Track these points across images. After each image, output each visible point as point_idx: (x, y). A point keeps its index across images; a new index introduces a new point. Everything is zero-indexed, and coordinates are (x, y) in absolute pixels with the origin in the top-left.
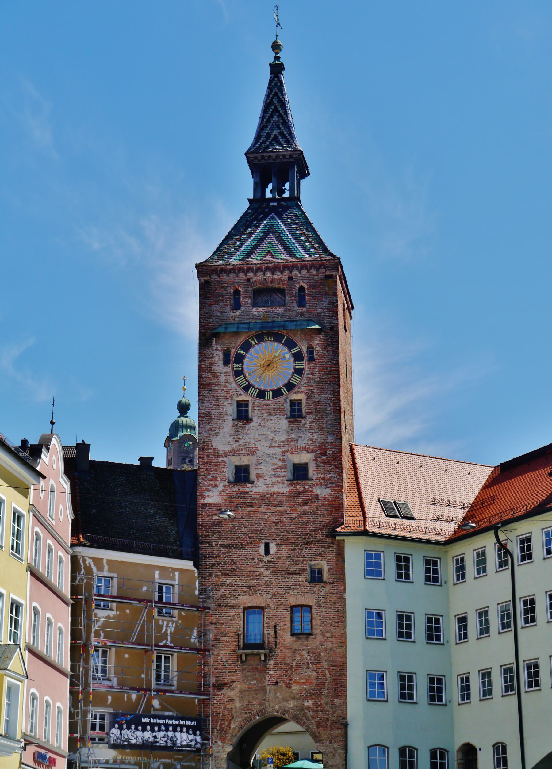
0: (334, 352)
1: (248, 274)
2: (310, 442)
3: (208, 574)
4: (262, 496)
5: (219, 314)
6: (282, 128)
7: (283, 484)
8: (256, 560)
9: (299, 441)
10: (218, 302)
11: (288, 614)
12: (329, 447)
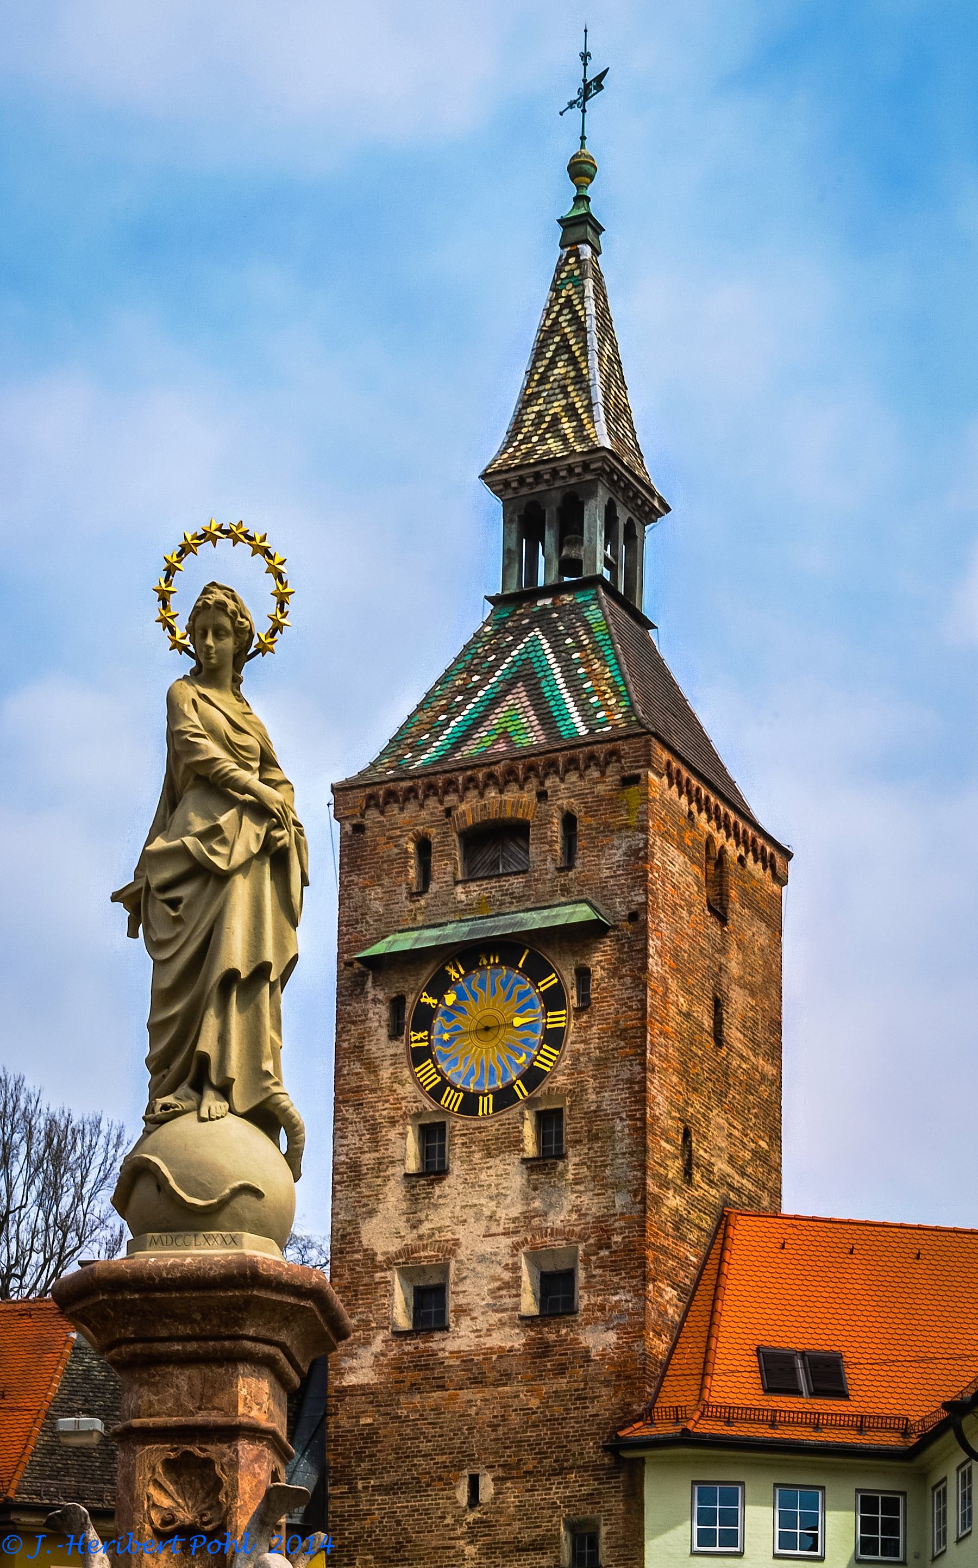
1: (447, 798)
2: (575, 1216)
3: (346, 1560)
4: (466, 1360)
7: (513, 1327)
8: (449, 1520)
9: (551, 1217)
10: (379, 878)
12: (617, 1224)
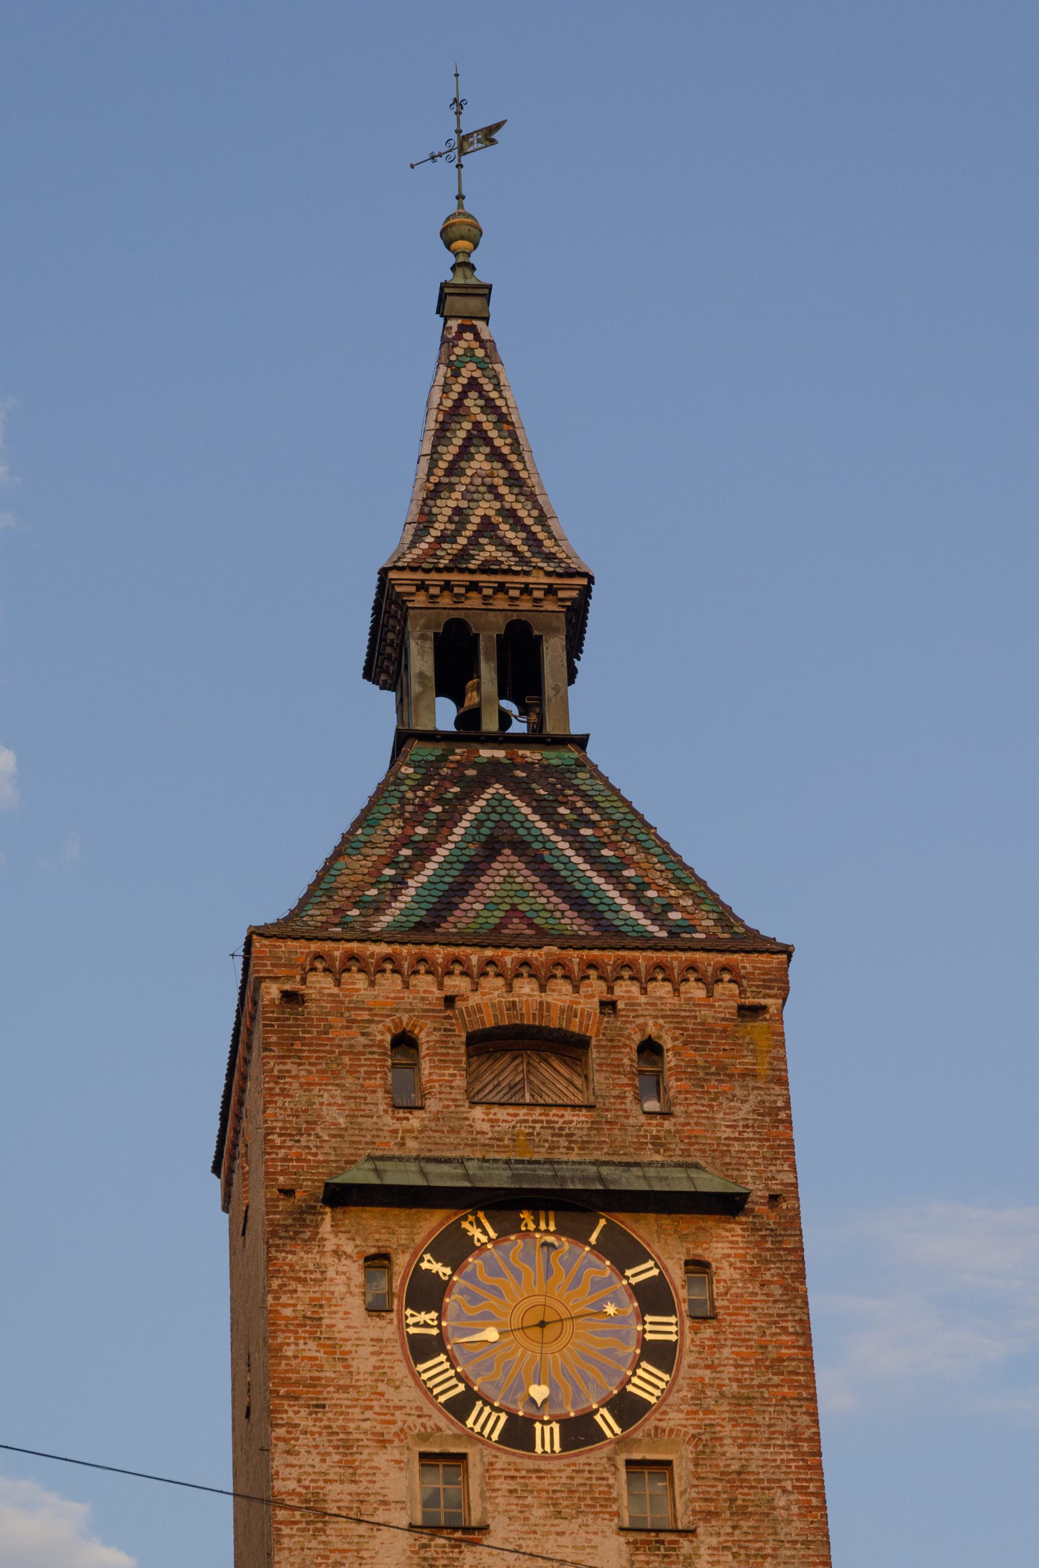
0: (786, 1288)
1: (448, 981)
5: (342, 1121)
6: (510, 498)
10: (336, 1074)
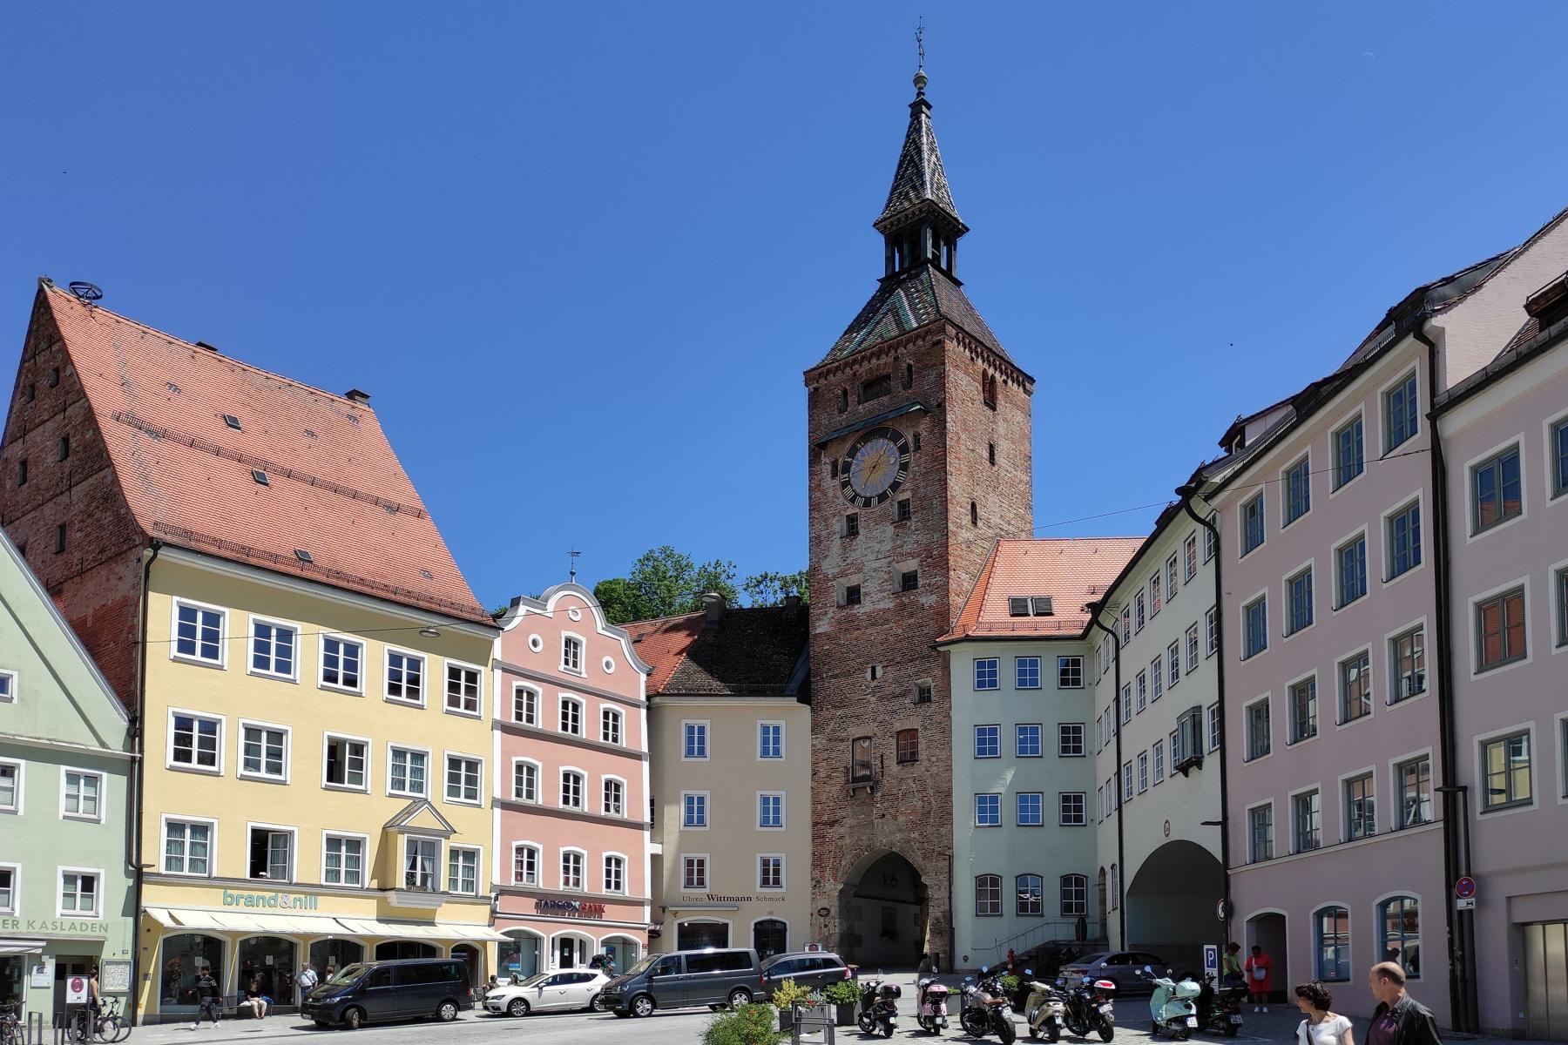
11: (894, 741)
